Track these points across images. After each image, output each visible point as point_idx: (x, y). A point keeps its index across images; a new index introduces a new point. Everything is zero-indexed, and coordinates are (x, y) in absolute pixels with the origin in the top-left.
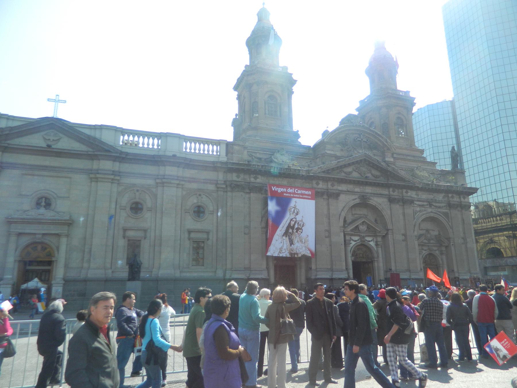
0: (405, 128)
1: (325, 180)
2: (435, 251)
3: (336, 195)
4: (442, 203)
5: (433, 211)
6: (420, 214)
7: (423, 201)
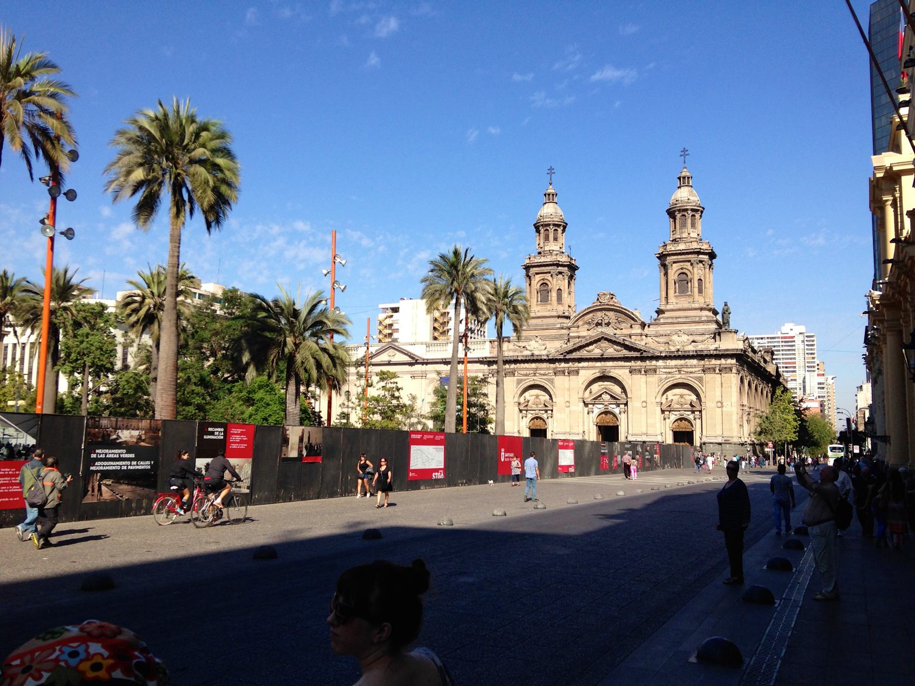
0: (689, 284)
1: (566, 361)
2: (688, 415)
3: (577, 372)
4: (695, 367)
5: (683, 376)
6: (667, 381)
7: (672, 368)
